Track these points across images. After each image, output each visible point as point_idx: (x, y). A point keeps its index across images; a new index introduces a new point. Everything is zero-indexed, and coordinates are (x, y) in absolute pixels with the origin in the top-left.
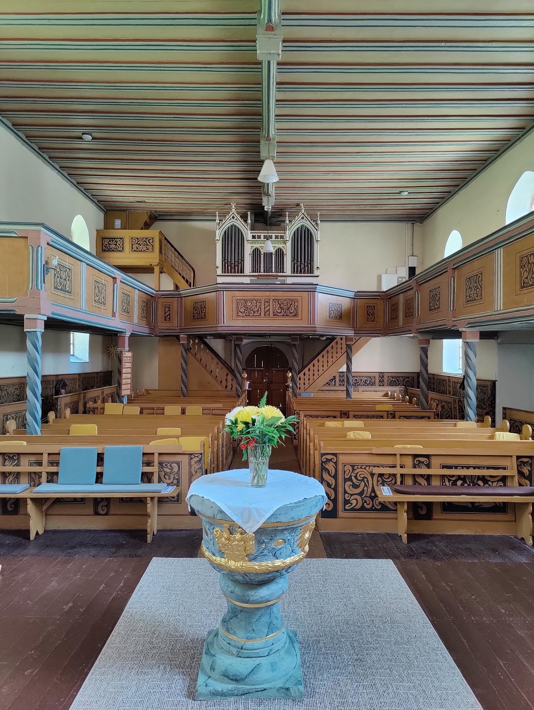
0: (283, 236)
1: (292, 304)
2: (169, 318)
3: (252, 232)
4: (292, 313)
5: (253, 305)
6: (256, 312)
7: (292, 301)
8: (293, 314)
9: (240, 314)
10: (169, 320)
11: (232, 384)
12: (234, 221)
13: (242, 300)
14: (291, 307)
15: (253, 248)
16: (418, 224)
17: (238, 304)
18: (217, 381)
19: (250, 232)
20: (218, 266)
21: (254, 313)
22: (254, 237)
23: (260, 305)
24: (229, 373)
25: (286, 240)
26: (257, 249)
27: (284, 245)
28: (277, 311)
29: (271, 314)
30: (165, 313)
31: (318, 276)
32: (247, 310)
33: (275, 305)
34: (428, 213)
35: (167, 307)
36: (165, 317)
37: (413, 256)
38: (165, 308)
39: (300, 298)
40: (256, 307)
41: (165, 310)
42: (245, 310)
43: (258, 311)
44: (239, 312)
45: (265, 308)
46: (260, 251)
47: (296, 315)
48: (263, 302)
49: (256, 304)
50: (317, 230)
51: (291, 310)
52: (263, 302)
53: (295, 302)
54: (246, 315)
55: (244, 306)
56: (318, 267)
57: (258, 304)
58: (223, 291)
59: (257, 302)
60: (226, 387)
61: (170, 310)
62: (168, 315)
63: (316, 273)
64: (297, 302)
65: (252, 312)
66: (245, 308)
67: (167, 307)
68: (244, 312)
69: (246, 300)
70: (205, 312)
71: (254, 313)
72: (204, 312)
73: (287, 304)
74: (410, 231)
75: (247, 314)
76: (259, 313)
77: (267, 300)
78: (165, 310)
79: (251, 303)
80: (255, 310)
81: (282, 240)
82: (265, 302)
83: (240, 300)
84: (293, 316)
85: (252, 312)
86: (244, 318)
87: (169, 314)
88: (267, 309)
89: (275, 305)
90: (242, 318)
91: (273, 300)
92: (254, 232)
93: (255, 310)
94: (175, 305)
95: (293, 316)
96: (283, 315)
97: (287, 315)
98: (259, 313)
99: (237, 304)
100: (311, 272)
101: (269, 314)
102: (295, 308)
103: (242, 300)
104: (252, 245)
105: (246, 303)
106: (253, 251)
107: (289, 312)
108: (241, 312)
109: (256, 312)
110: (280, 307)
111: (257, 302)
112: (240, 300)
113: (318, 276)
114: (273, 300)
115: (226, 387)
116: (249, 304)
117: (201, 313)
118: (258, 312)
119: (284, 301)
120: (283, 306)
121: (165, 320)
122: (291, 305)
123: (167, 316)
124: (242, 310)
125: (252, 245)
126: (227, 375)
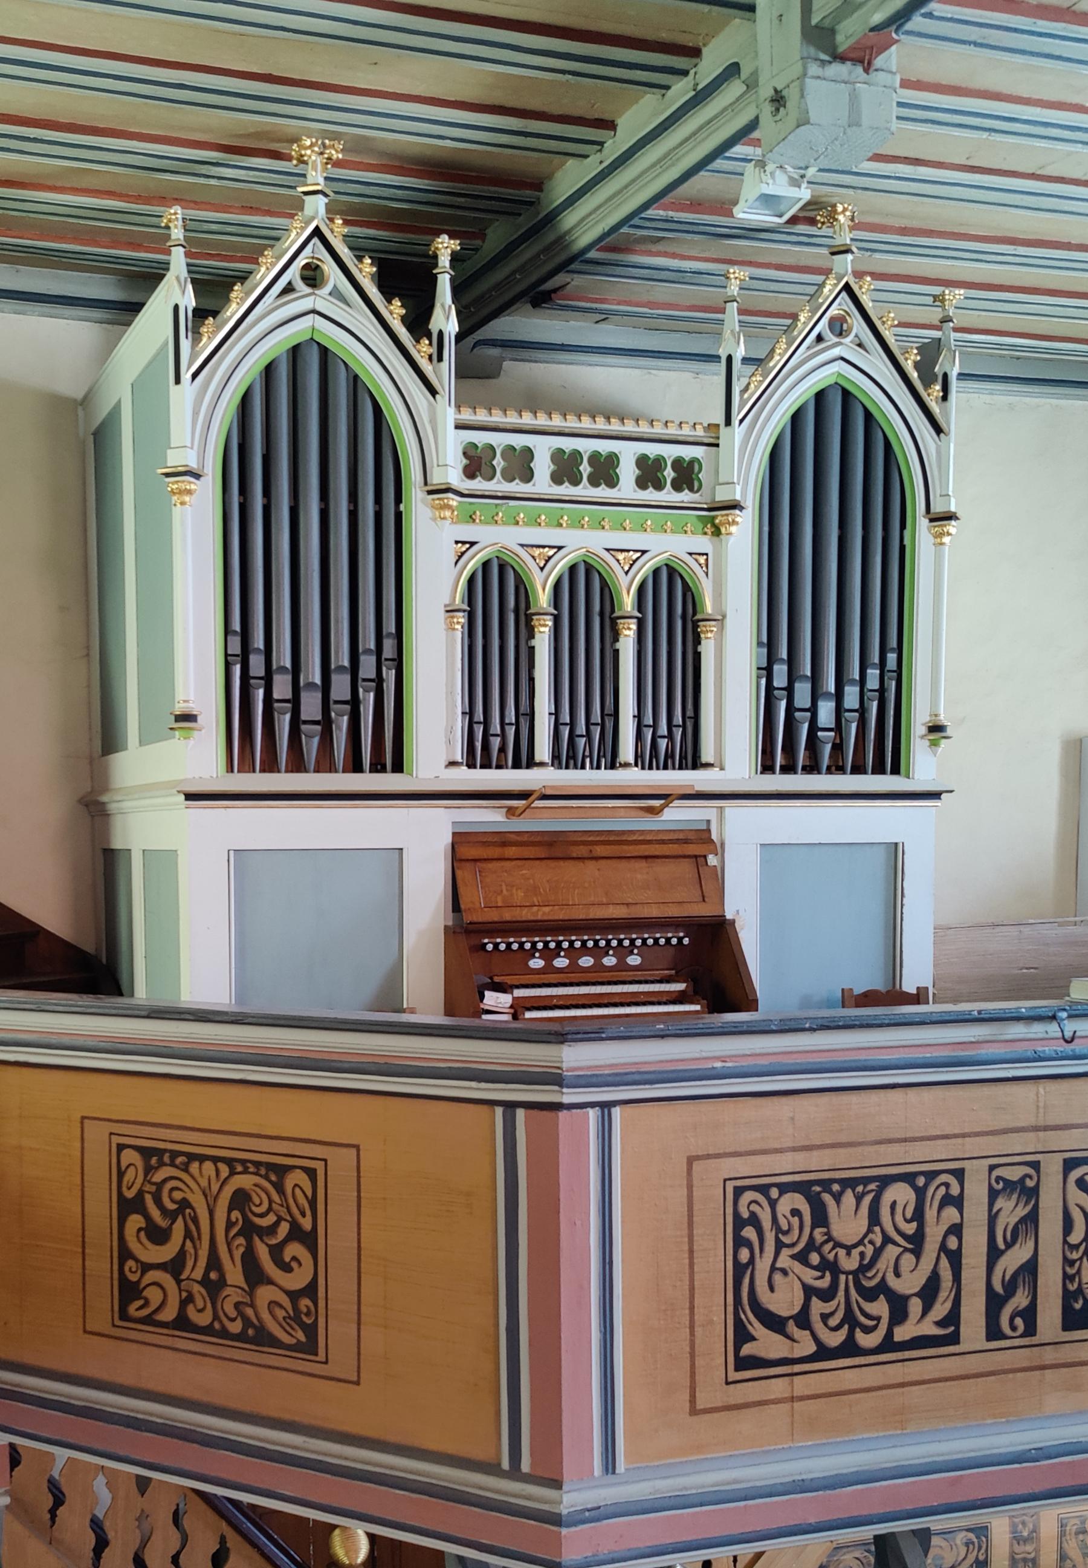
3: (467, 416)
6: (915, 1306)
13: (784, 1188)
17: (749, 1232)
20: (193, 708)
21: (899, 1313)
23: (956, 1230)
27: (703, 543)
29: (1050, 1315)
32: (827, 1295)
40: (917, 1253)
43: (929, 1292)
44: (757, 1328)
49: (919, 1215)
55: (802, 1257)
56: (943, 719)
57: (930, 1214)
58: (606, 1106)
59: (920, 1193)
65: (880, 1308)
66: (809, 1276)
69: (826, 1184)
75: (834, 1339)
76: (941, 1309)
77: (1014, 1174)
80: (909, 1283)
81: (685, 497)
83: (763, 1189)
85: (880, 1308)
86: (802, 1386)
88: (1014, 1259)
90: (778, 1388)
92: (482, 416)
93: (909, 1283)
98: (941, 1309)
99: (740, 1242)
101: (1029, 1315)
103: (784, 1188)
104: (468, 532)
105: (820, 1217)
109: (915, 1306)
111: (920, 1193)
112: (763, 1189)
118: (926, 1310)
125: (468, 532)
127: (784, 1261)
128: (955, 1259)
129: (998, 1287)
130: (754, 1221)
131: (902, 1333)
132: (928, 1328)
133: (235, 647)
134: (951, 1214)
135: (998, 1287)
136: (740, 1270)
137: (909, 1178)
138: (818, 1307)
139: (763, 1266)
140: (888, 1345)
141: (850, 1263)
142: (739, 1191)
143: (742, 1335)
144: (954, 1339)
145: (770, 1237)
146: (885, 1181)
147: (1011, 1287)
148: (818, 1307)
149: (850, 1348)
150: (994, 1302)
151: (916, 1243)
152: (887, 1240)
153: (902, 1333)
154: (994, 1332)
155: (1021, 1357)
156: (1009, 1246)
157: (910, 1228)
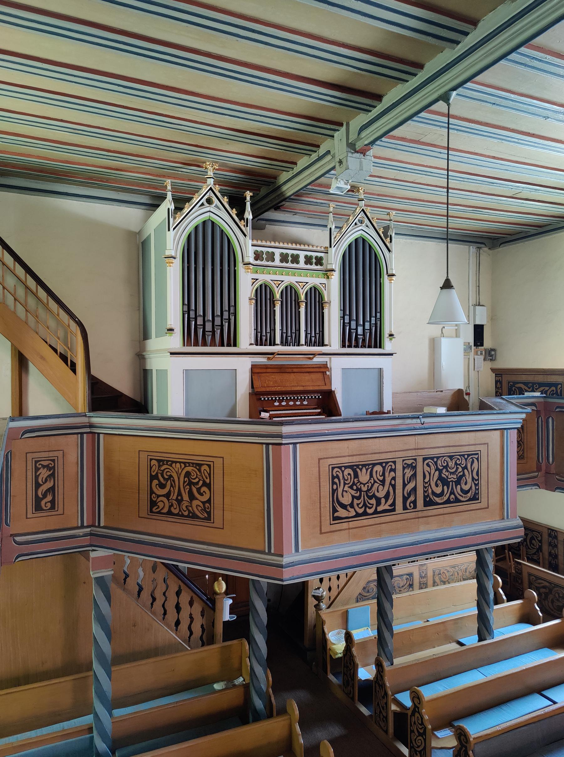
0: (321, 258)
1: (466, 467)
2: (53, 502)
3: (255, 242)
4: (466, 492)
5: (375, 482)
6: (383, 501)
7: (466, 459)
8: (469, 495)
9: (342, 513)
10: (53, 507)
11: (191, 614)
12: (212, 210)
13: (346, 467)
14: (464, 475)
15: (257, 285)
16: (486, 249)
17: (336, 480)
18: (154, 613)
19: (250, 242)
20: (173, 327)
22: (258, 256)
24: (183, 586)
25: (329, 267)
26: (266, 286)
28: (433, 492)
30: (38, 485)
31: (392, 354)
32: (358, 498)
33: (430, 474)
34: (526, 232)
35: (44, 467)
36: (38, 501)
37: (479, 305)
38: (37, 469)
39: (483, 448)
40: (383, 485)
41: (37, 477)
42: (353, 497)
43: (387, 497)
44: (339, 508)
45: (404, 485)
46: (271, 291)
47: (475, 498)
48: (399, 467)
49: (383, 474)
50: (389, 251)
51: (466, 484)
52: (399, 467)
53: (473, 462)
54: (358, 515)
55: (351, 487)
57: (387, 474)
58: (295, 444)
60: (178, 623)
61: (54, 473)
62: (48, 490)
63: (388, 346)
64: (477, 459)
65: (373, 501)
66: (353, 492)
67: (44, 467)
68: (352, 505)
69: (358, 466)
70: (209, 501)
71: (379, 503)
72: (205, 498)
73: (457, 468)
74: (473, 260)
75: (361, 511)
76: (390, 501)
78: (37, 477)
79: (371, 476)
82: (404, 468)
83: (340, 468)
84: (470, 500)
85: (373, 501)
87: (52, 490)
89: (430, 474)
91: (424, 459)
94: (73, 456)
95: (470, 500)
96: (448, 502)
97: (457, 500)
98: (390, 501)
99: (334, 483)
100: (378, 344)
101: (415, 502)
102: (473, 478)
103: (346, 467)
105: (356, 476)
106: (257, 290)
107: (462, 490)
108: (344, 506)
109: (383, 501)
110: (440, 478)
111: (384, 468)
112: (340, 468)
113: (392, 354)
114: (424, 459)
115: (178, 623)
116: (364, 477)
117: (186, 497)
119: (448, 459)
120: (447, 474)
121: (38, 508)
122: (466, 471)
123: (45, 496)
124: (346, 500)
126: (178, 593)
127: (346, 488)
128: (394, 487)
129: (406, 495)
130: (338, 477)
131: (380, 509)
132: (387, 507)
133: (186, 308)
134: (392, 474)
135: (406, 495)
136: (334, 491)
137: (381, 464)
138: (356, 501)
139: (340, 490)
140: (376, 512)
141: (365, 489)
142: (333, 468)
143: (335, 510)
144: (394, 510)
145: (342, 481)
146: (374, 465)
147: (409, 495)
148: (356, 501)
149: (365, 514)
150: (405, 499)
151: (383, 482)
152: (375, 482)
153: (380, 509)
154: (405, 508)
155: (413, 515)
156: (408, 483)
157: (381, 478)
